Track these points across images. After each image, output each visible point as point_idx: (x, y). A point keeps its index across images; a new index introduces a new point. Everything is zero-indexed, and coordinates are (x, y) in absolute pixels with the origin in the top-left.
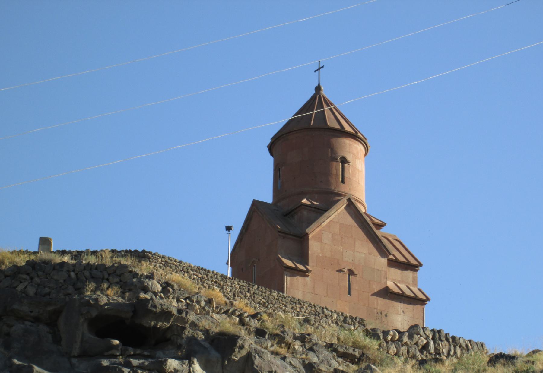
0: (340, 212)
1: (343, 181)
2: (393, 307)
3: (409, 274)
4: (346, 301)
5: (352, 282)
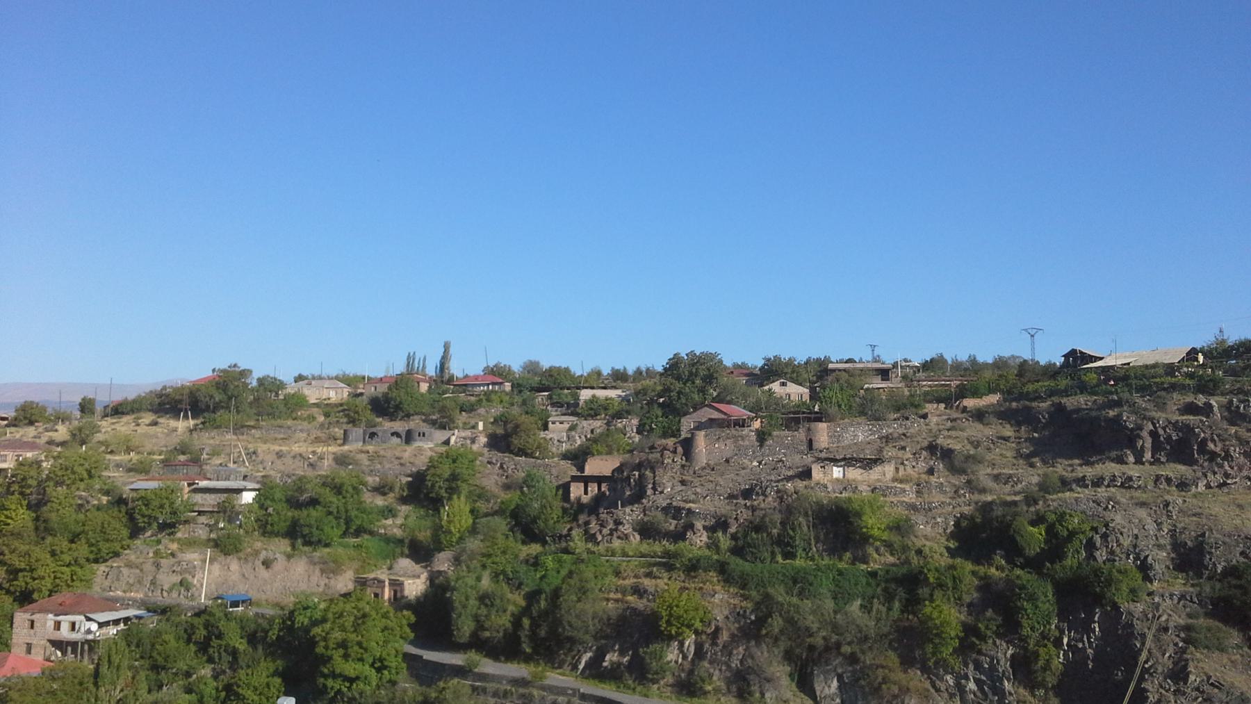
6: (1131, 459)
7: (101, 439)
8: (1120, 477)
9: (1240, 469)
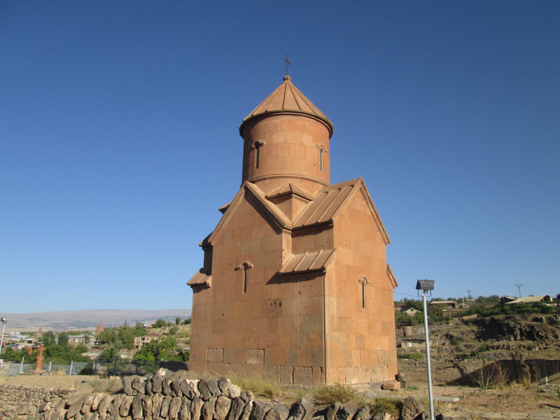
0: (241, 204)
1: (258, 167)
2: (288, 290)
3: (324, 234)
4: (241, 301)
5: (247, 277)
6: (512, 338)
7: (179, 333)
8: (506, 345)
9: (553, 342)
